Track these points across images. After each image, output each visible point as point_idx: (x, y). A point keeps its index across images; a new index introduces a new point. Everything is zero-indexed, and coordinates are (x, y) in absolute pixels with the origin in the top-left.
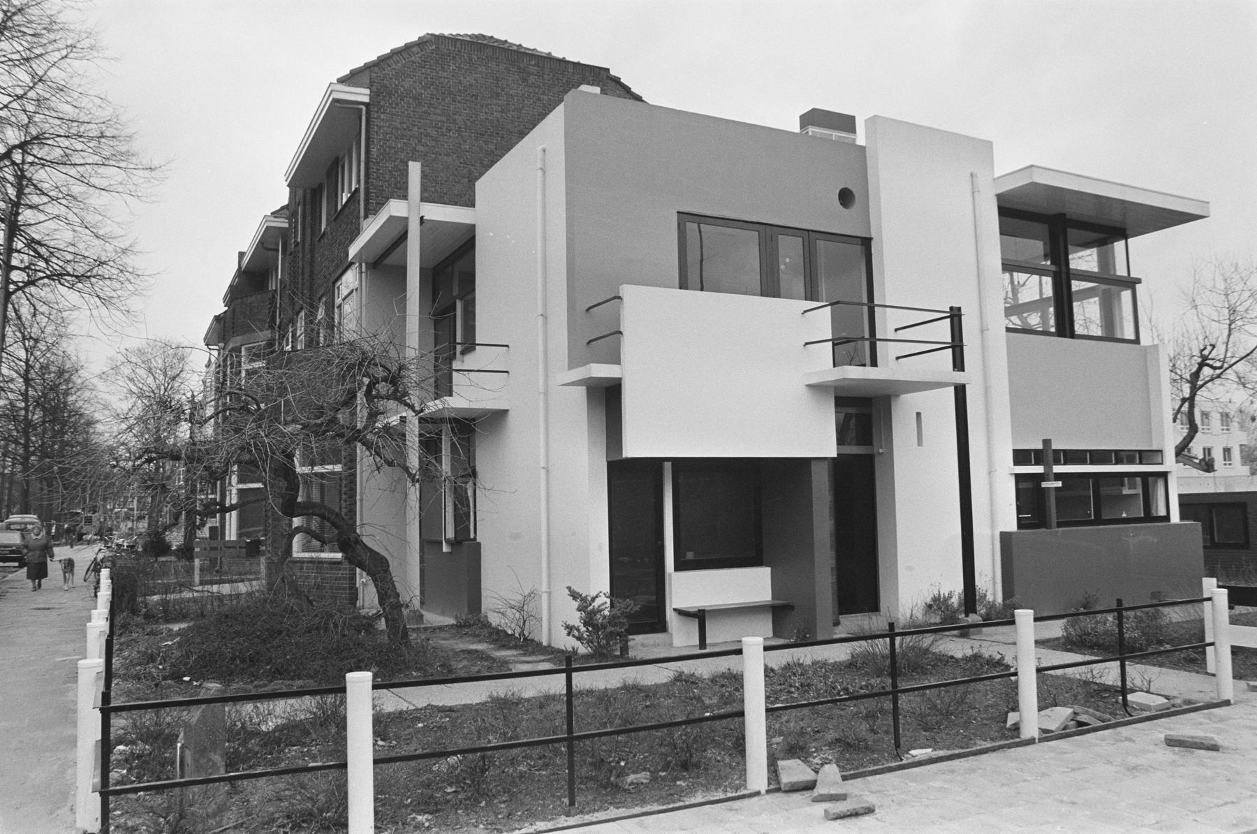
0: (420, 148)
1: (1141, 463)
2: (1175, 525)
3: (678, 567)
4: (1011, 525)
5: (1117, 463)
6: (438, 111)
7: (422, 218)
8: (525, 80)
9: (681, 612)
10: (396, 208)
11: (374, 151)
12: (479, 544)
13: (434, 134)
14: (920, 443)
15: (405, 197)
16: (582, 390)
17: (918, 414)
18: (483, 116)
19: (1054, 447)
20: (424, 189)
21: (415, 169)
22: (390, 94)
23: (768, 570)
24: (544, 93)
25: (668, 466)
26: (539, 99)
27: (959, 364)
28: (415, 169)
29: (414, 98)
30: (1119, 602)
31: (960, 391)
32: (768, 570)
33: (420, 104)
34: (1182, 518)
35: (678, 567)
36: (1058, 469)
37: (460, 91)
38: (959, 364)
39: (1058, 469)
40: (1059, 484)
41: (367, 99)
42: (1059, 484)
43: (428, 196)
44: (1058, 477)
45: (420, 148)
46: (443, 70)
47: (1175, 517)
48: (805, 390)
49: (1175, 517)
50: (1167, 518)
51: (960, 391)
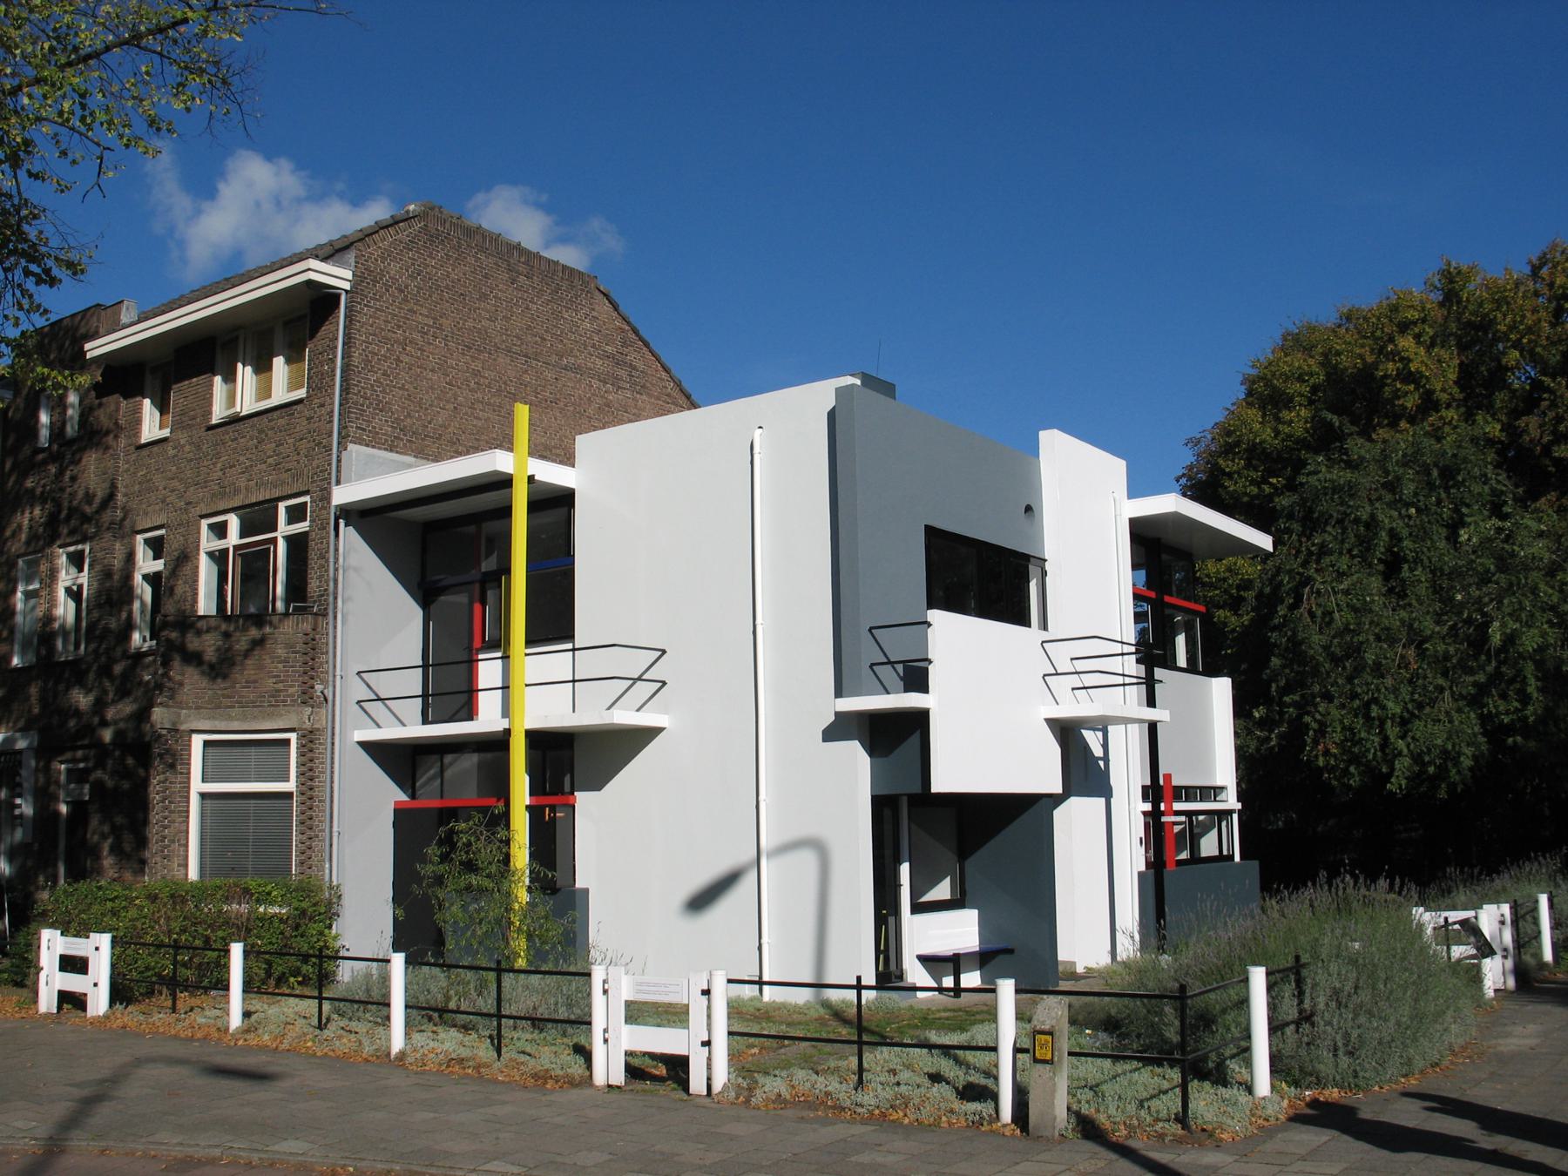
3: (917, 908)
4: (1143, 868)
6: (425, 312)
8: (513, 281)
9: (923, 959)
11: (356, 361)
13: (417, 336)
15: (511, 450)
18: (470, 324)
19: (1175, 782)
21: (522, 412)
22: (375, 281)
23: (976, 912)
25: (904, 800)
27: (1151, 702)
28: (522, 412)
30: (859, 978)
31: (1153, 727)
32: (976, 912)
33: (406, 300)
34: (1242, 858)
36: (1177, 806)
38: (1151, 702)
39: (1177, 806)
41: (347, 286)
42: (1183, 818)
44: (1178, 813)
47: (1237, 858)
49: (1237, 858)
50: (1231, 857)
51: (1153, 727)
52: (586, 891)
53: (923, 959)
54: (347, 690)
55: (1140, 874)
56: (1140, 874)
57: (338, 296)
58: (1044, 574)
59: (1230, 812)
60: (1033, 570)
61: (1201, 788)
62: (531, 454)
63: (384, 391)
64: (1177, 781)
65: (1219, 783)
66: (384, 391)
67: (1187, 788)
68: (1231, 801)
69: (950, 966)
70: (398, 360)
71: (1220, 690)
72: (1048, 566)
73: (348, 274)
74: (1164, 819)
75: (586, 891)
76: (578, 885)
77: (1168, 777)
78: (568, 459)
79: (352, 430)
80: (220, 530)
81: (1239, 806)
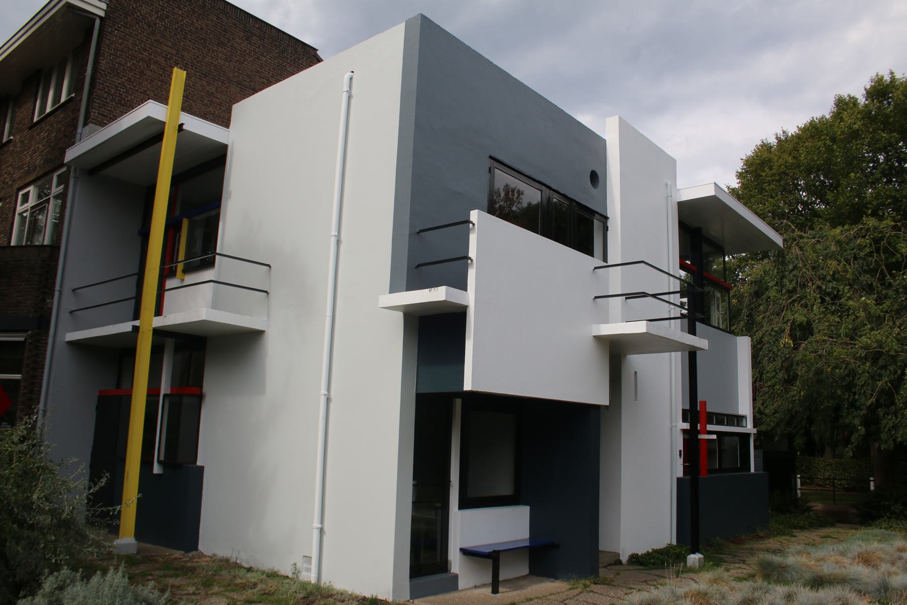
0: (148, 73)
1: (738, 426)
2: (753, 474)
3: (464, 504)
5: (727, 425)
6: (170, 44)
7: (181, 126)
9: (465, 552)
10: (151, 109)
11: (103, 63)
12: (202, 468)
14: (636, 399)
16: (400, 315)
17: (636, 373)
19: (708, 410)
20: (186, 97)
21: (179, 77)
24: (262, 55)
26: (258, 58)
28: (179, 77)
29: (149, 26)
31: (692, 355)
35: (461, 507)
36: (710, 427)
37: (191, 31)
39: (710, 427)
40: (714, 437)
41: (102, 14)
42: (714, 437)
43: (188, 107)
45: (148, 73)
46: (178, 7)
48: (590, 344)
52: (202, 468)
53: (465, 552)
54: (63, 302)
55: (679, 479)
56: (679, 479)
57: (94, 20)
58: (606, 229)
59: (748, 435)
60: (597, 224)
61: (728, 416)
62: (183, 109)
63: (127, 92)
64: (710, 409)
65: (741, 413)
66: (127, 92)
67: (717, 414)
68: (749, 427)
69: (490, 562)
70: (142, 73)
71: (743, 345)
72: (610, 224)
73: (104, 6)
74: (701, 437)
75: (202, 468)
76: (199, 463)
77: (704, 404)
78: (225, 121)
79: (94, 113)
80: (26, 198)
81: (755, 431)
